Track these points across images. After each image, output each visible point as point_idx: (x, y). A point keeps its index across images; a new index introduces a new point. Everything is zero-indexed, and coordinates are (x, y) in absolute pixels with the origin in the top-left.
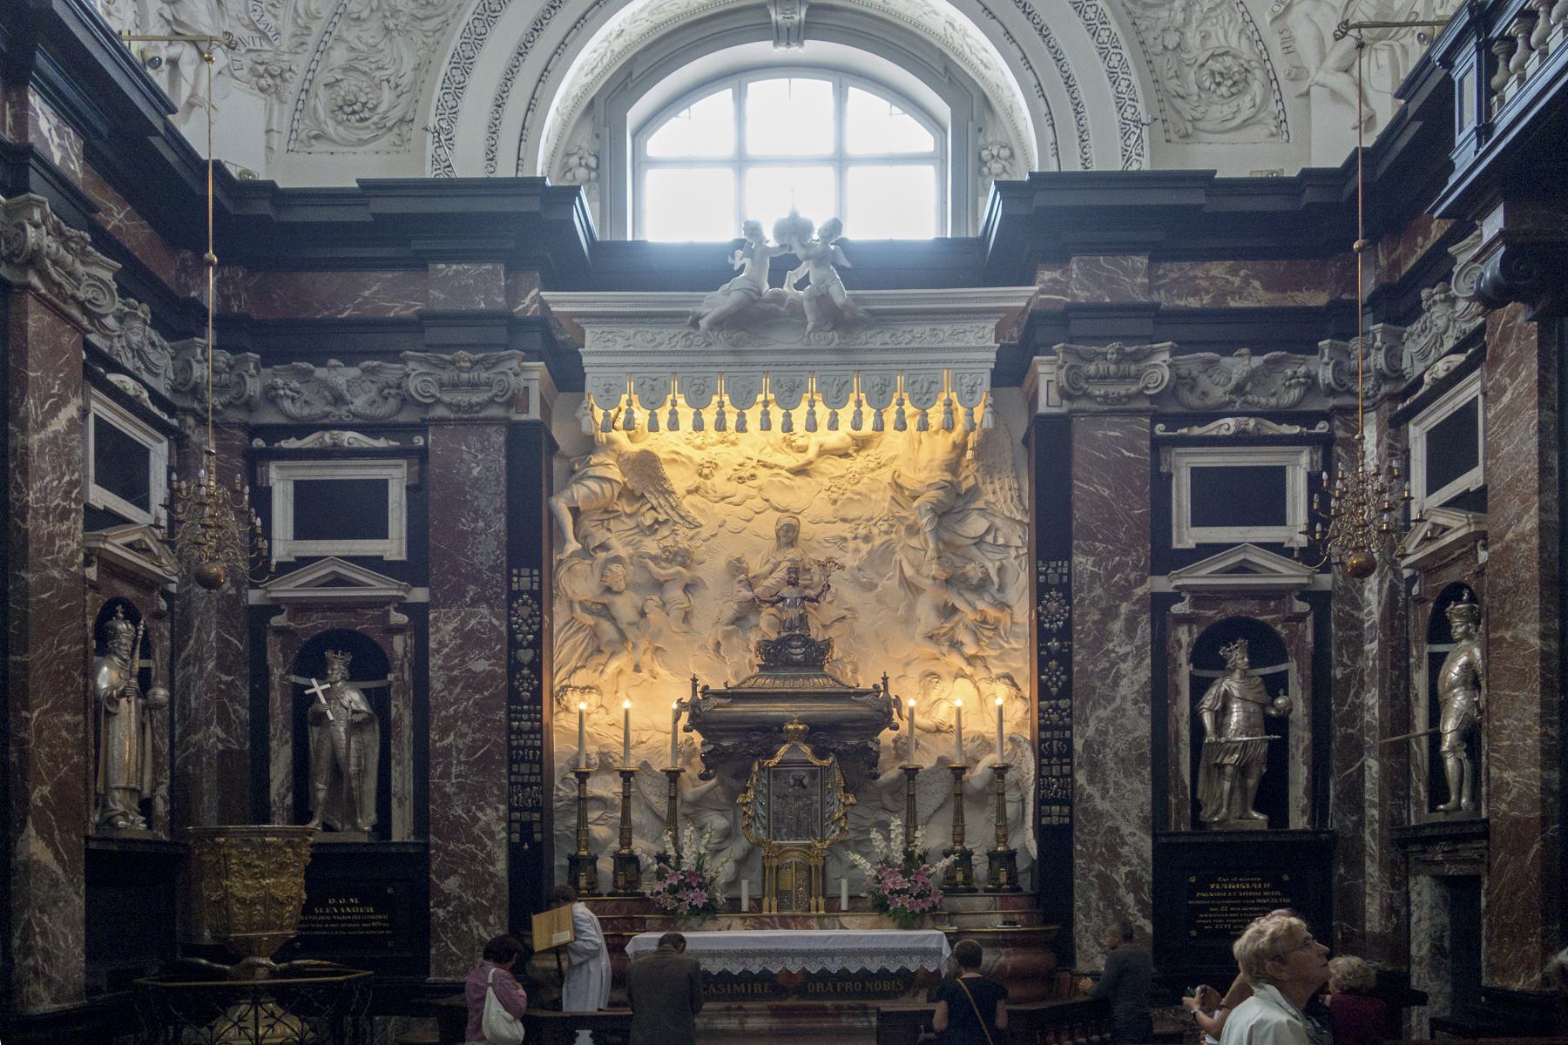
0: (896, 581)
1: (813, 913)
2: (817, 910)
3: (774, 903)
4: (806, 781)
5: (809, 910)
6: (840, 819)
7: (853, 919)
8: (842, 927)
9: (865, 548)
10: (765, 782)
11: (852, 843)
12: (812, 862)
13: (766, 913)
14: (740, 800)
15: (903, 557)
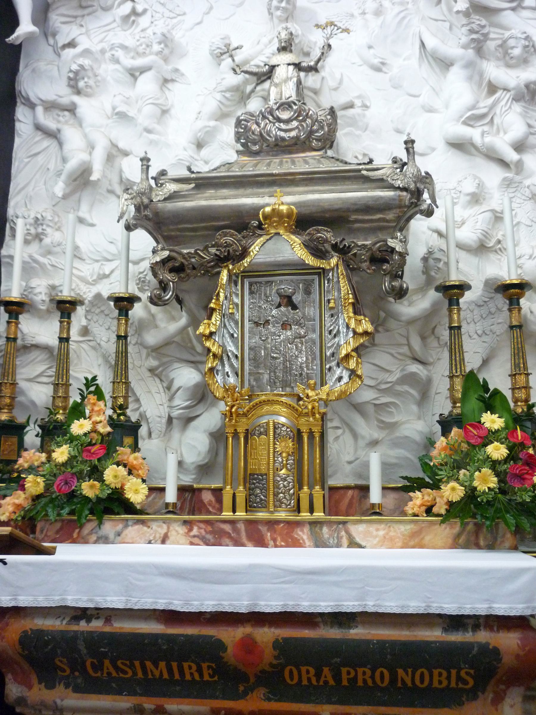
0: (414, 61)
1: (305, 515)
2: (311, 510)
3: (241, 493)
4: (297, 298)
5: (298, 510)
6: (348, 356)
7: (372, 528)
8: (353, 544)
9: (374, 23)
10: (238, 301)
11: (371, 409)
12: (304, 424)
13: (227, 514)
14: (201, 329)
15: (423, 29)
